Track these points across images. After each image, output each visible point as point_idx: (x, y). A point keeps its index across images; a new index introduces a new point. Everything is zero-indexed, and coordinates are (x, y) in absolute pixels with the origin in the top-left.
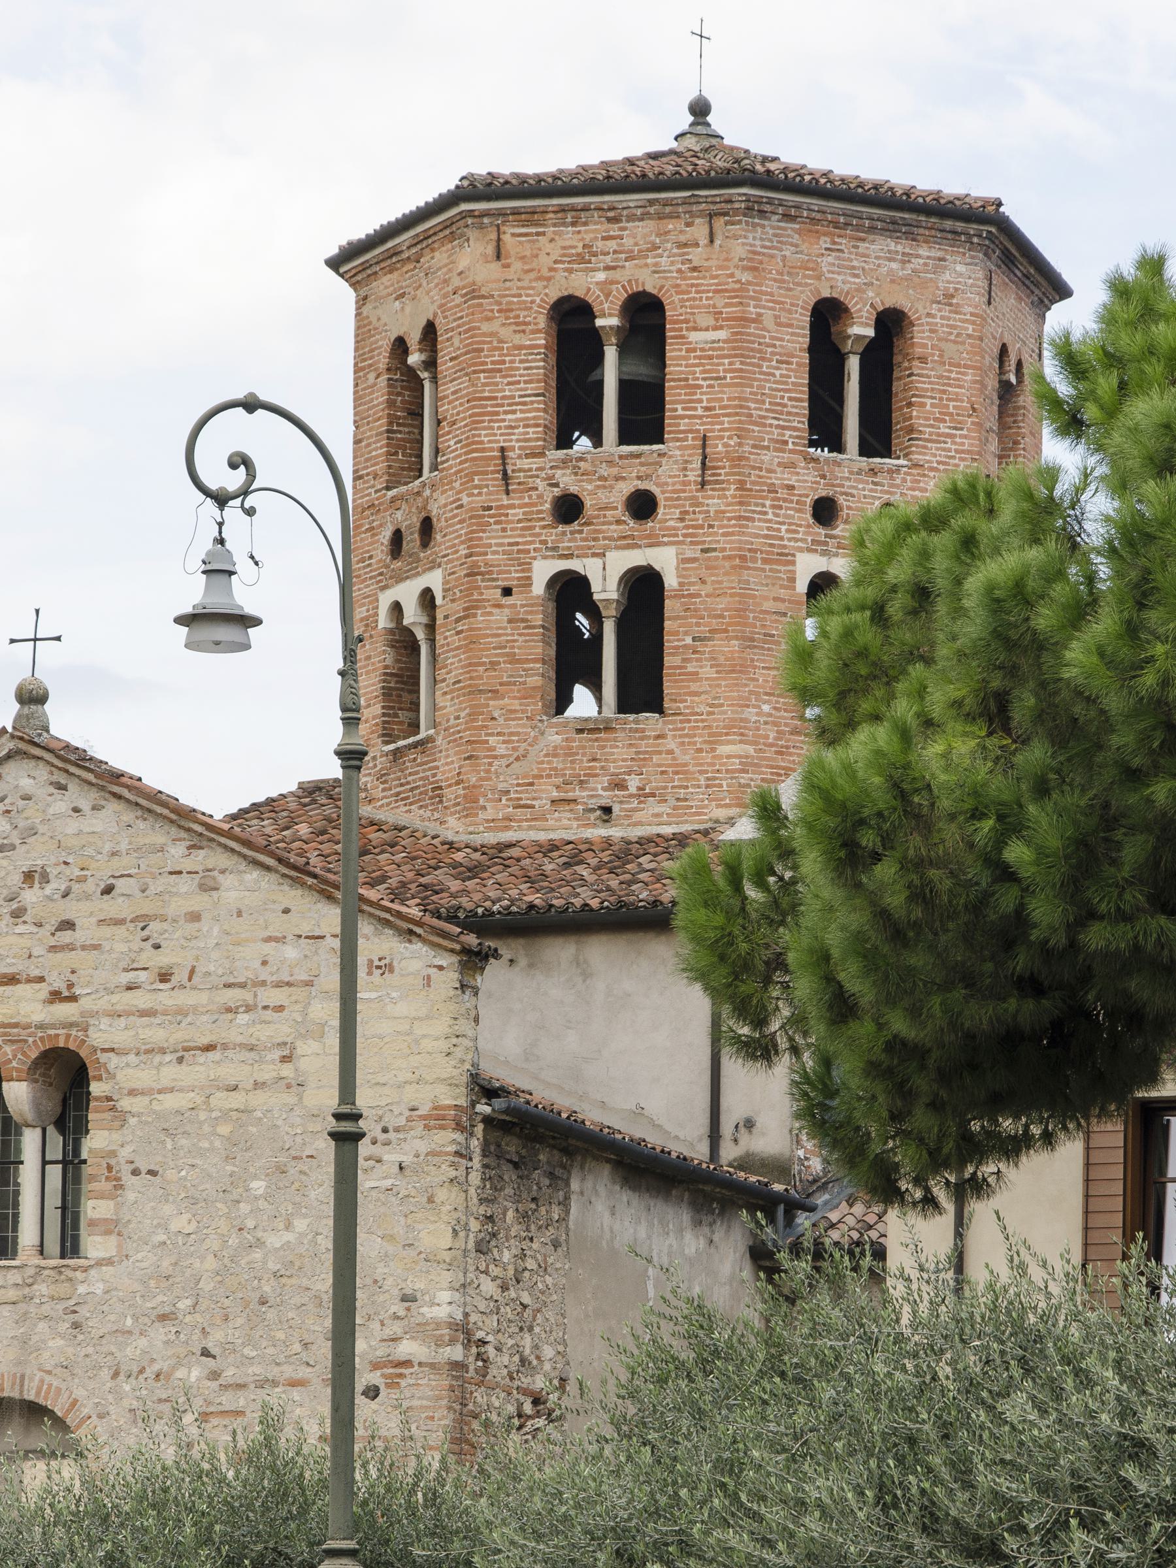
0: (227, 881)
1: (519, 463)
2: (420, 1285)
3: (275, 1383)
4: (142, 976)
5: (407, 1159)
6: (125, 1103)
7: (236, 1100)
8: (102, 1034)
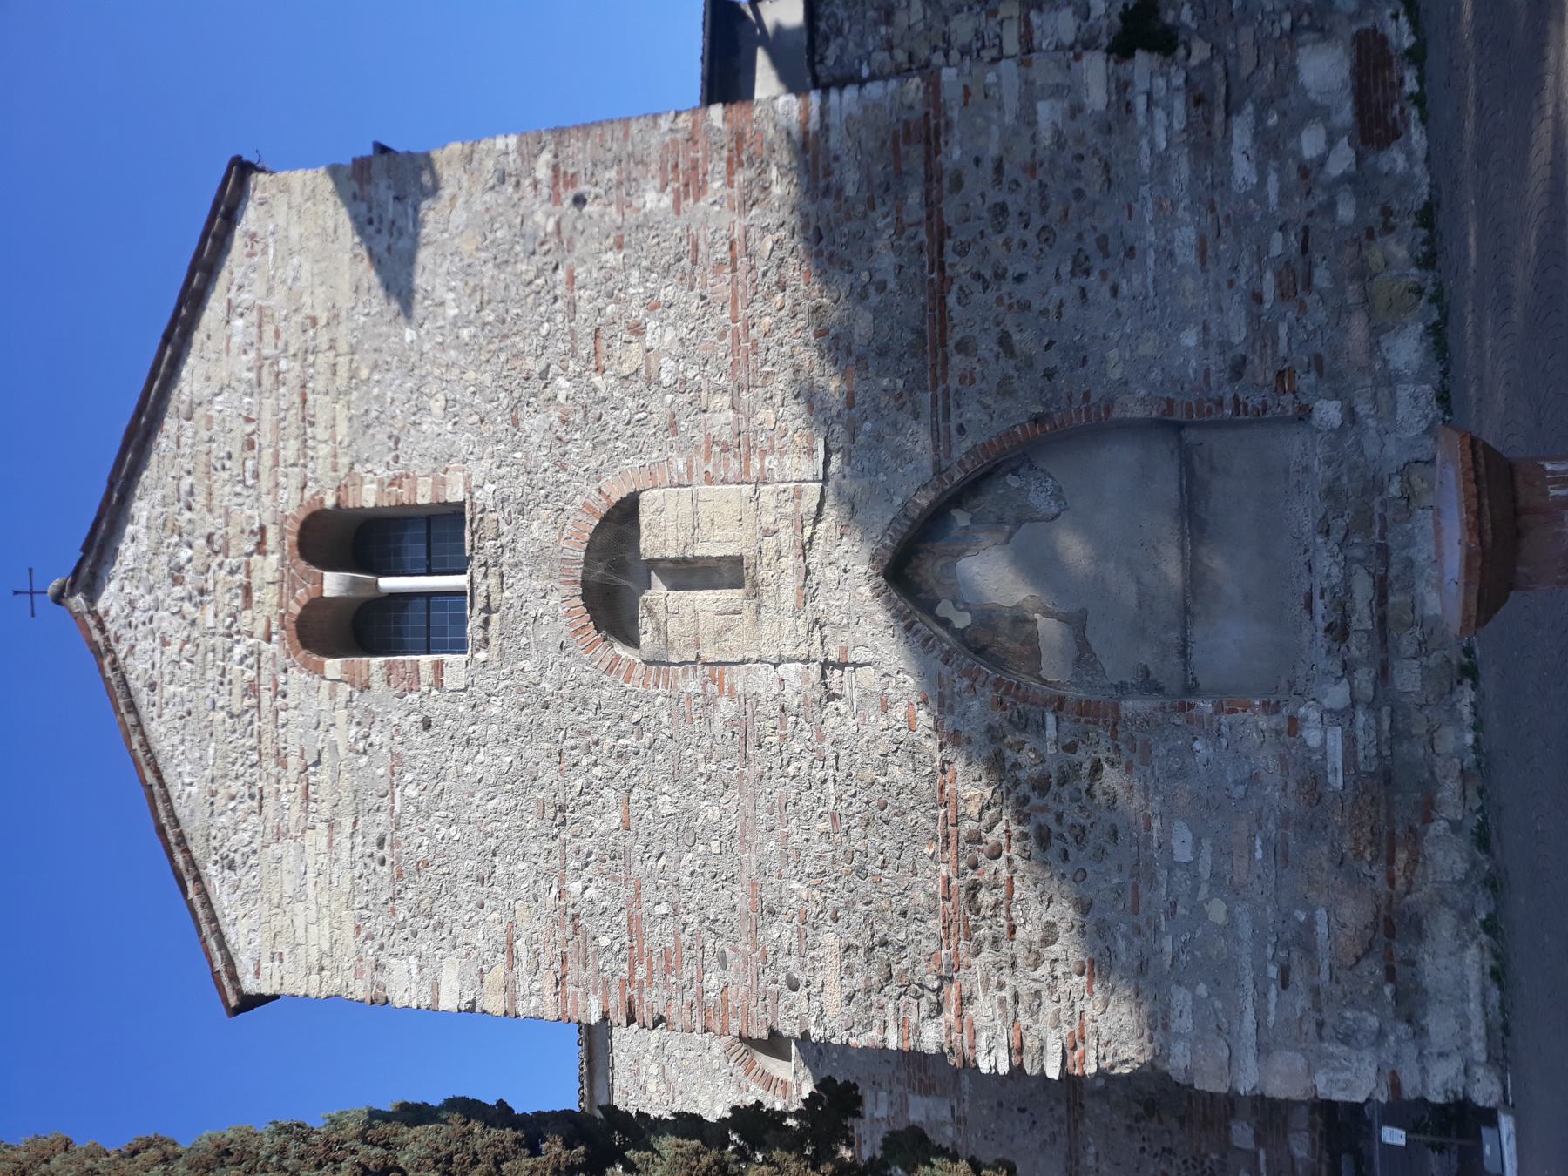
2: (489, 164)
4: (249, 464)
5: (392, 193)
8: (293, 503)
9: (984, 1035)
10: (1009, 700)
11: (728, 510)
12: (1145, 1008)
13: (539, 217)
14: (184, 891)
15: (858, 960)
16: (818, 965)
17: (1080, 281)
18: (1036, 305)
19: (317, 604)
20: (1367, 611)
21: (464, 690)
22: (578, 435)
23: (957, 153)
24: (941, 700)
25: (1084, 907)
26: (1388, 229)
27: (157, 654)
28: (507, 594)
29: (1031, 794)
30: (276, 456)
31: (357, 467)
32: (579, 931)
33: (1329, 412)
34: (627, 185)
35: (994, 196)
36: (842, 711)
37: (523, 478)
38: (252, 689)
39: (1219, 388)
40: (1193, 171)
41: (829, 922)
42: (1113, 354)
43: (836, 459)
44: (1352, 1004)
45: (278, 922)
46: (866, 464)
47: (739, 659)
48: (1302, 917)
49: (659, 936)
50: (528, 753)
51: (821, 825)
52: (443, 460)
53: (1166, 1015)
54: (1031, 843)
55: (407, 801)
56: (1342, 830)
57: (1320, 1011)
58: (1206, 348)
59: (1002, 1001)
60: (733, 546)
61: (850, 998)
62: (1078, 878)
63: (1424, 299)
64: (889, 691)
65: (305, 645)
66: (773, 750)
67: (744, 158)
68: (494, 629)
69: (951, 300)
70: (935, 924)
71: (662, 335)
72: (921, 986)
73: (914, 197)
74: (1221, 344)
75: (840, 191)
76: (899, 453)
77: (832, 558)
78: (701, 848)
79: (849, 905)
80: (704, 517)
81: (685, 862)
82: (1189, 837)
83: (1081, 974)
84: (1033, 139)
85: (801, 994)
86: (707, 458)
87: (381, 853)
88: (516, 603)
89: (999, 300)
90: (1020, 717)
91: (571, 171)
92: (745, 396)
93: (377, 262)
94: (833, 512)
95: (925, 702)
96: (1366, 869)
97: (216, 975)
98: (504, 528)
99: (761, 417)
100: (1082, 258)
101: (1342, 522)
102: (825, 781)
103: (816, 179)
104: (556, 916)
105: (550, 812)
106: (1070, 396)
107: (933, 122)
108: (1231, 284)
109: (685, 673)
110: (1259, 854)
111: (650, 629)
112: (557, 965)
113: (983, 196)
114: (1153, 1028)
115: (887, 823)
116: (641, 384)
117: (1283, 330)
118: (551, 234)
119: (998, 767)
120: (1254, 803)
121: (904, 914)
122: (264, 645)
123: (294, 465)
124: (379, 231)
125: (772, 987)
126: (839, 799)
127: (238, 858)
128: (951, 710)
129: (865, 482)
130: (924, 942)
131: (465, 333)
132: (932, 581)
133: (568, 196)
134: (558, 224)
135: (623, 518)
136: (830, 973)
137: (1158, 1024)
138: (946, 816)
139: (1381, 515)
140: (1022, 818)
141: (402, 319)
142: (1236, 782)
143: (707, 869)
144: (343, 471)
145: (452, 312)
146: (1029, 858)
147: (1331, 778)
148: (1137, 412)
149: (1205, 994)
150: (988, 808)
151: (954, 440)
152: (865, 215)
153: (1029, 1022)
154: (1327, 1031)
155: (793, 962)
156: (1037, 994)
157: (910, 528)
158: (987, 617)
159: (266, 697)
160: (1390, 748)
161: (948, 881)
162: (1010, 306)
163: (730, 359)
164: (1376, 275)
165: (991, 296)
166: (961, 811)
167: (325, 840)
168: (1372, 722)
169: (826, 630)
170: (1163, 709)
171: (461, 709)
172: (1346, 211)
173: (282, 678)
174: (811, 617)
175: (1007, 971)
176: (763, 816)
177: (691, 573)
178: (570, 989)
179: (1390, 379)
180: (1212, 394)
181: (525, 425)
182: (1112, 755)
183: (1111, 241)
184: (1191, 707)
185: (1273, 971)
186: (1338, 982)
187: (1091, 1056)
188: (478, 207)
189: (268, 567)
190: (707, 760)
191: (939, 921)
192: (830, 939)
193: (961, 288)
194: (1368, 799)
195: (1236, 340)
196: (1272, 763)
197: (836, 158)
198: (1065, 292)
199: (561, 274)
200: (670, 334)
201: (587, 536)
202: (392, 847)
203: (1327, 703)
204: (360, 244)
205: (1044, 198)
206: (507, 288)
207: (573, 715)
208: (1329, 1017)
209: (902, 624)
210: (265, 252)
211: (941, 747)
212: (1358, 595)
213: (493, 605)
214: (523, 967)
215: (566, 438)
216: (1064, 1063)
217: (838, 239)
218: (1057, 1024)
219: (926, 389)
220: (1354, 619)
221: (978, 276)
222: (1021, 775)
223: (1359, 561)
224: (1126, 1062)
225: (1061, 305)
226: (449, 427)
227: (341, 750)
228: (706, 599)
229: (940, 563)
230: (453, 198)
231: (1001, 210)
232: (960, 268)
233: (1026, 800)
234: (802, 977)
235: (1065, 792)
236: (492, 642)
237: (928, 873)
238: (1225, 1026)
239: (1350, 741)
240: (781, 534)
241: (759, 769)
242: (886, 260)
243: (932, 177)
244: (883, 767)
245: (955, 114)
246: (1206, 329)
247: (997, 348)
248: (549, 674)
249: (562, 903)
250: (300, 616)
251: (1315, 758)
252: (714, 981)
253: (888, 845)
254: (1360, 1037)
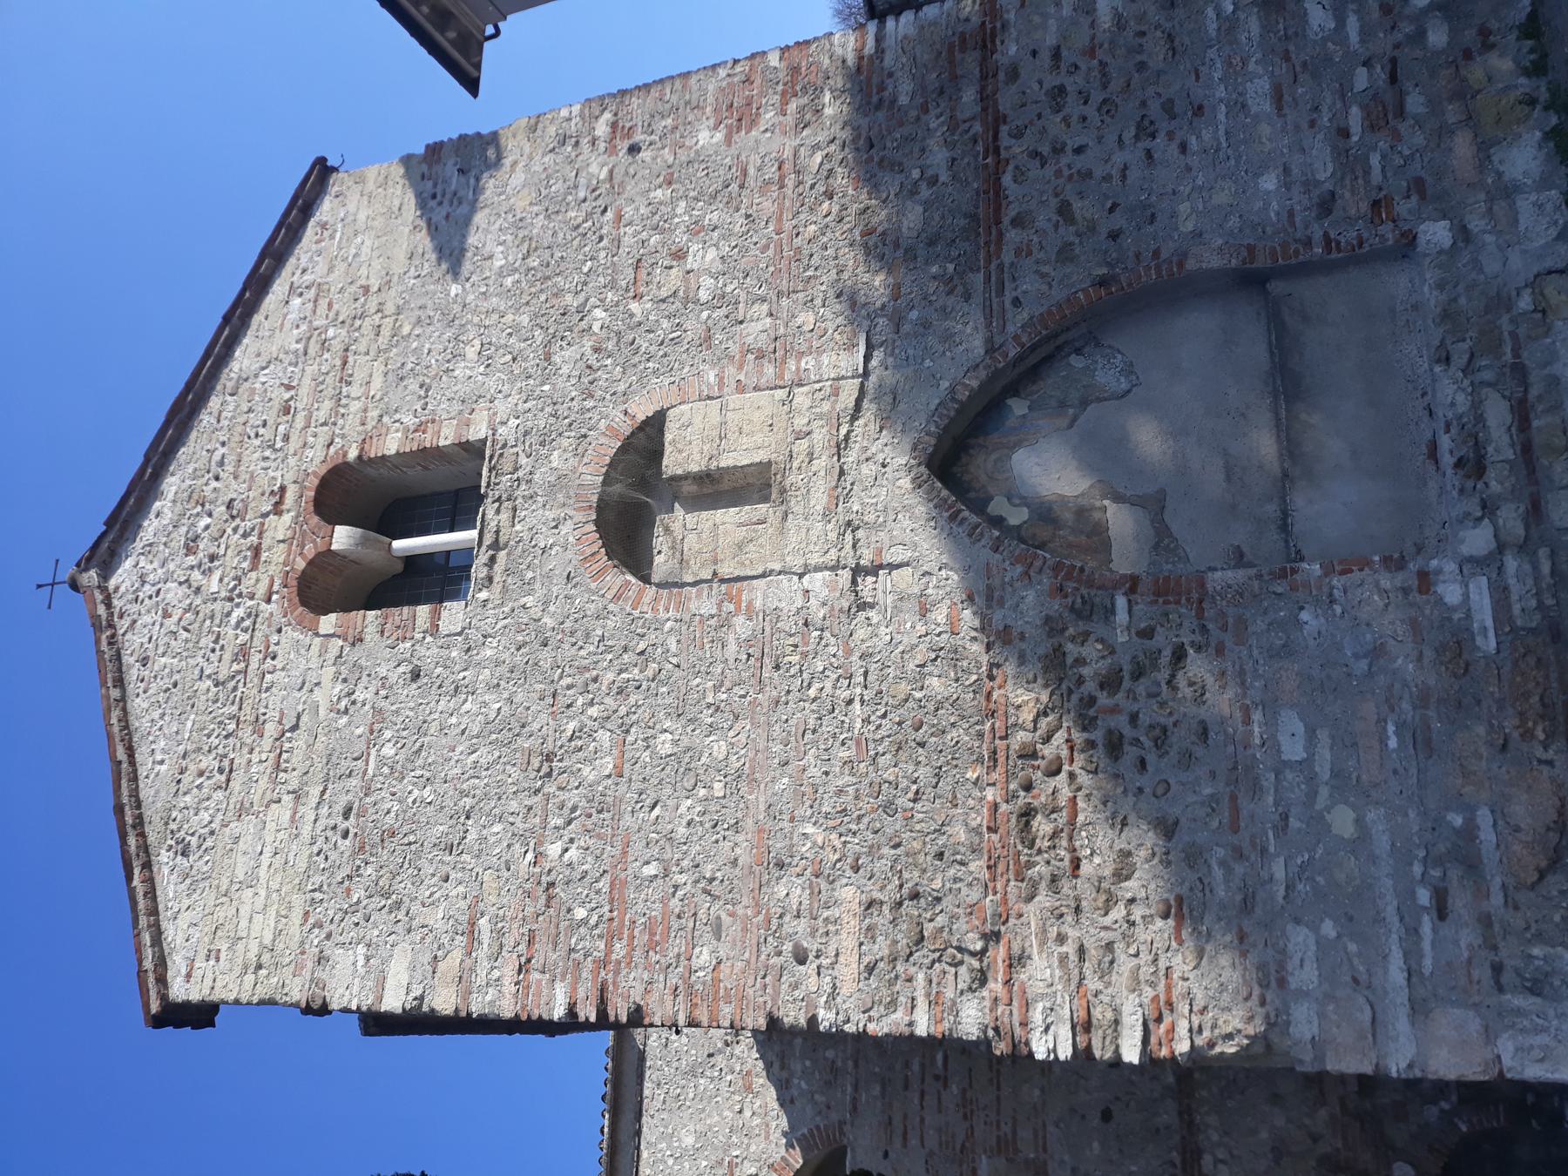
2: (552, 130)
4: (281, 429)
8: (316, 460)
9: (1040, 1006)
10: (1070, 586)
11: (757, 417)
12: (1252, 958)
13: (594, 169)
14: (129, 877)
15: (882, 918)
16: (832, 928)
17: (1147, 143)
18: (1098, 172)
19: (325, 561)
20: (1506, 439)
21: (459, 634)
22: (609, 361)
23: (1013, 49)
24: (985, 595)
25: (1167, 828)
26: (1487, 47)
27: (157, 627)
28: (518, 527)
29: (1098, 694)
30: (309, 418)
31: (385, 419)
32: (553, 903)
33: (1436, 233)
34: (681, 130)
35: (1051, 81)
36: (874, 621)
37: (548, 409)
38: (243, 653)
39: (1306, 228)
40: (1263, 27)
41: (849, 873)
42: (1184, 208)
43: (878, 355)
44: (1539, 937)
45: (220, 914)
46: (911, 352)
47: (760, 571)
48: (1458, 821)
50: (518, 698)
51: (844, 754)
52: (468, 403)
53: (1281, 967)
54: (1099, 753)
55: (382, 761)
56: (1501, 704)
57: (1495, 948)
58: (1288, 189)
59: (1063, 959)
60: (761, 452)
61: (870, 969)
62: (1160, 791)
63: (1539, 107)
64: (930, 591)
65: (304, 603)
66: (792, 671)
67: (798, 88)
68: (498, 568)
69: (1007, 180)
70: (978, 866)
71: (702, 257)
72: (960, 949)
73: (969, 95)
74: (1306, 183)
75: (894, 101)
76: (947, 337)
77: (869, 454)
78: (702, 792)
79: (873, 850)
80: (732, 426)
81: (682, 810)
82: (1300, 728)
83: (1165, 916)
84: (1093, 25)
85: (810, 968)
86: (741, 368)
87: (343, 825)
88: (526, 536)
89: (1058, 173)
90: (1084, 602)
91: (628, 125)
92: (785, 302)
93: (433, 229)
94: (873, 407)
95: (970, 598)
96: (1539, 752)
97: (141, 973)
98: (523, 460)
99: (799, 321)
100: (1146, 123)
101: (1465, 346)
102: (850, 702)
103: (870, 95)
104: (528, 886)
105: (536, 763)
106: (1138, 255)
107: (989, 27)
108: (1312, 124)
109: (699, 595)
110: (1393, 743)
111: (665, 548)
112: (522, 948)
113: (1040, 83)
114: (1265, 985)
115: (922, 745)
116: (678, 304)
117: (1375, 160)
118: (604, 181)
119: (1055, 669)
120: (1382, 680)
121: (940, 856)
122: (263, 606)
123: (324, 424)
124: (440, 203)
125: (774, 960)
126: (867, 721)
127: (194, 841)
128: (1001, 603)
129: (909, 371)
130: (965, 891)
131: (509, 281)
132: (983, 478)
134: (611, 172)
135: (647, 440)
136: (847, 940)
137: (1271, 980)
138: (993, 728)
139: (1510, 333)
140: (1086, 724)
141: (449, 277)
142: (1356, 656)
143: (707, 818)
144: (371, 424)
145: (499, 263)
146: (1095, 772)
147: (1479, 641)
148: (1215, 262)
149: (1333, 934)
150: (1046, 714)
151: (1009, 315)
152: (918, 119)
153: (1099, 986)
154: (1507, 977)
155: (802, 926)
156: (1109, 946)
157: (957, 411)
158: (1044, 513)
159: (255, 659)
160: (1554, 596)
161: (995, 806)
162: (1070, 177)
163: (771, 269)
164: (1479, 91)
165: (1049, 170)
166: (1012, 720)
167: (289, 813)
168: (1527, 567)
169: (860, 534)
170: (1259, 576)
171: (454, 654)
172: (1438, 37)
173: (274, 638)
174: (842, 518)
175: (1069, 919)
176: (777, 748)
177: (717, 488)
178: (535, 976)
179: (1508, 191)
180: (1298, 235)
181: (557, 359)
182: (1198, 638)
183: (1177, 102)
184: (1294, 571)
185: (1424, 896)
186: (1516, 908)
187: (1182, 1028)
188: (538, 168)
190: (716, 688)
191: (983, 863)
192: (849, 893)
193: (1017, 167)
194: (1532, 660)
195: (1321, 176)
196: (1400, 630)
197: (891, 75)
198: (1131, 156)
199: (610, 215)
200: (712, 254)
201: (607, 460)
202: (358, 816)
203: (1465, 550)
204: (421, 216)
205: (1104, 75)
206: (554, 234)
207: (573, 651)
208: (1509, 953)
209: (946, 515)
210: (332, 237)
211: (989, 647)
212: (1492, 422)
213: (502, 540)
214: (483, 952)
215: (596, 365)
216: (1146, 1041)
217: (889, 144)
218: (1135, 987)
219: (978, 270)
220: (1490, 449)
221: (1035, 154)
222: (1086, 671)
223: (1489, 385)
224: (1229, 1036)
225: (1126, 167)
226: (482, 369)
227: (322, 712)
228: (727, 517)
229: (994, 457)
230: (515, 163)
231: (1061, 90)
232: (1015, 149)
233: (1092, 700)
234: (811, 945)
235: (1141, 688)
236: (496, 579)
237: (971, 802)
238: (1363, 978)
239: (1501, 595)
240: (814, 435)
241: (775, 693)
242: (938, 156)
243: (987, 75)
244: (919, 681)
245: (1012, 16)
246: (1286, 170)
247: (1055, 218)
248: (552, 608)
249: (537, 870)
250: (303, 572)
251: (1456, 616)
252: (705, 957)
253: (924, 773)
254: (1557, 983)
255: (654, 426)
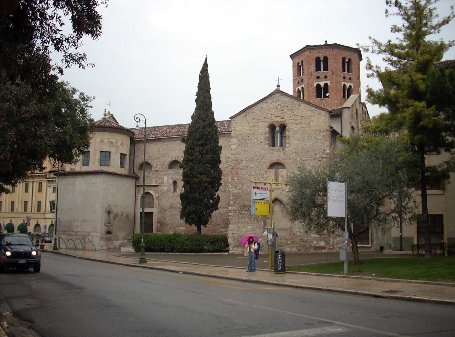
0: (302, 105)
1: (313, 73)
3: (308, 160)
6: (290, 129)
7: (303, 129)
8: (287, 122)
13: (318, 156)
38: (265, 118)
49: (240, 172)
133: (320, 159)
136: (237, 191)
159: (264, 120)
189: (279, 119)
255: (285, 168)
